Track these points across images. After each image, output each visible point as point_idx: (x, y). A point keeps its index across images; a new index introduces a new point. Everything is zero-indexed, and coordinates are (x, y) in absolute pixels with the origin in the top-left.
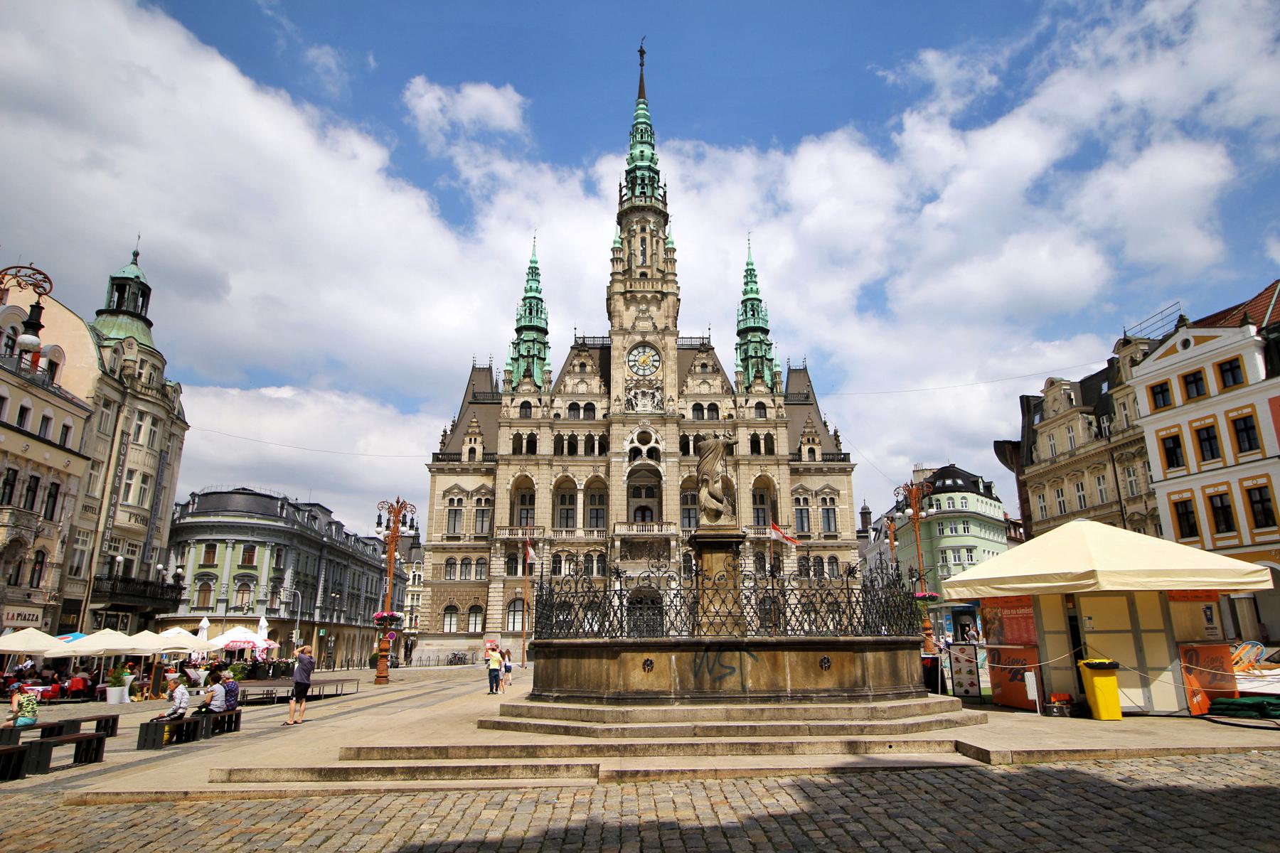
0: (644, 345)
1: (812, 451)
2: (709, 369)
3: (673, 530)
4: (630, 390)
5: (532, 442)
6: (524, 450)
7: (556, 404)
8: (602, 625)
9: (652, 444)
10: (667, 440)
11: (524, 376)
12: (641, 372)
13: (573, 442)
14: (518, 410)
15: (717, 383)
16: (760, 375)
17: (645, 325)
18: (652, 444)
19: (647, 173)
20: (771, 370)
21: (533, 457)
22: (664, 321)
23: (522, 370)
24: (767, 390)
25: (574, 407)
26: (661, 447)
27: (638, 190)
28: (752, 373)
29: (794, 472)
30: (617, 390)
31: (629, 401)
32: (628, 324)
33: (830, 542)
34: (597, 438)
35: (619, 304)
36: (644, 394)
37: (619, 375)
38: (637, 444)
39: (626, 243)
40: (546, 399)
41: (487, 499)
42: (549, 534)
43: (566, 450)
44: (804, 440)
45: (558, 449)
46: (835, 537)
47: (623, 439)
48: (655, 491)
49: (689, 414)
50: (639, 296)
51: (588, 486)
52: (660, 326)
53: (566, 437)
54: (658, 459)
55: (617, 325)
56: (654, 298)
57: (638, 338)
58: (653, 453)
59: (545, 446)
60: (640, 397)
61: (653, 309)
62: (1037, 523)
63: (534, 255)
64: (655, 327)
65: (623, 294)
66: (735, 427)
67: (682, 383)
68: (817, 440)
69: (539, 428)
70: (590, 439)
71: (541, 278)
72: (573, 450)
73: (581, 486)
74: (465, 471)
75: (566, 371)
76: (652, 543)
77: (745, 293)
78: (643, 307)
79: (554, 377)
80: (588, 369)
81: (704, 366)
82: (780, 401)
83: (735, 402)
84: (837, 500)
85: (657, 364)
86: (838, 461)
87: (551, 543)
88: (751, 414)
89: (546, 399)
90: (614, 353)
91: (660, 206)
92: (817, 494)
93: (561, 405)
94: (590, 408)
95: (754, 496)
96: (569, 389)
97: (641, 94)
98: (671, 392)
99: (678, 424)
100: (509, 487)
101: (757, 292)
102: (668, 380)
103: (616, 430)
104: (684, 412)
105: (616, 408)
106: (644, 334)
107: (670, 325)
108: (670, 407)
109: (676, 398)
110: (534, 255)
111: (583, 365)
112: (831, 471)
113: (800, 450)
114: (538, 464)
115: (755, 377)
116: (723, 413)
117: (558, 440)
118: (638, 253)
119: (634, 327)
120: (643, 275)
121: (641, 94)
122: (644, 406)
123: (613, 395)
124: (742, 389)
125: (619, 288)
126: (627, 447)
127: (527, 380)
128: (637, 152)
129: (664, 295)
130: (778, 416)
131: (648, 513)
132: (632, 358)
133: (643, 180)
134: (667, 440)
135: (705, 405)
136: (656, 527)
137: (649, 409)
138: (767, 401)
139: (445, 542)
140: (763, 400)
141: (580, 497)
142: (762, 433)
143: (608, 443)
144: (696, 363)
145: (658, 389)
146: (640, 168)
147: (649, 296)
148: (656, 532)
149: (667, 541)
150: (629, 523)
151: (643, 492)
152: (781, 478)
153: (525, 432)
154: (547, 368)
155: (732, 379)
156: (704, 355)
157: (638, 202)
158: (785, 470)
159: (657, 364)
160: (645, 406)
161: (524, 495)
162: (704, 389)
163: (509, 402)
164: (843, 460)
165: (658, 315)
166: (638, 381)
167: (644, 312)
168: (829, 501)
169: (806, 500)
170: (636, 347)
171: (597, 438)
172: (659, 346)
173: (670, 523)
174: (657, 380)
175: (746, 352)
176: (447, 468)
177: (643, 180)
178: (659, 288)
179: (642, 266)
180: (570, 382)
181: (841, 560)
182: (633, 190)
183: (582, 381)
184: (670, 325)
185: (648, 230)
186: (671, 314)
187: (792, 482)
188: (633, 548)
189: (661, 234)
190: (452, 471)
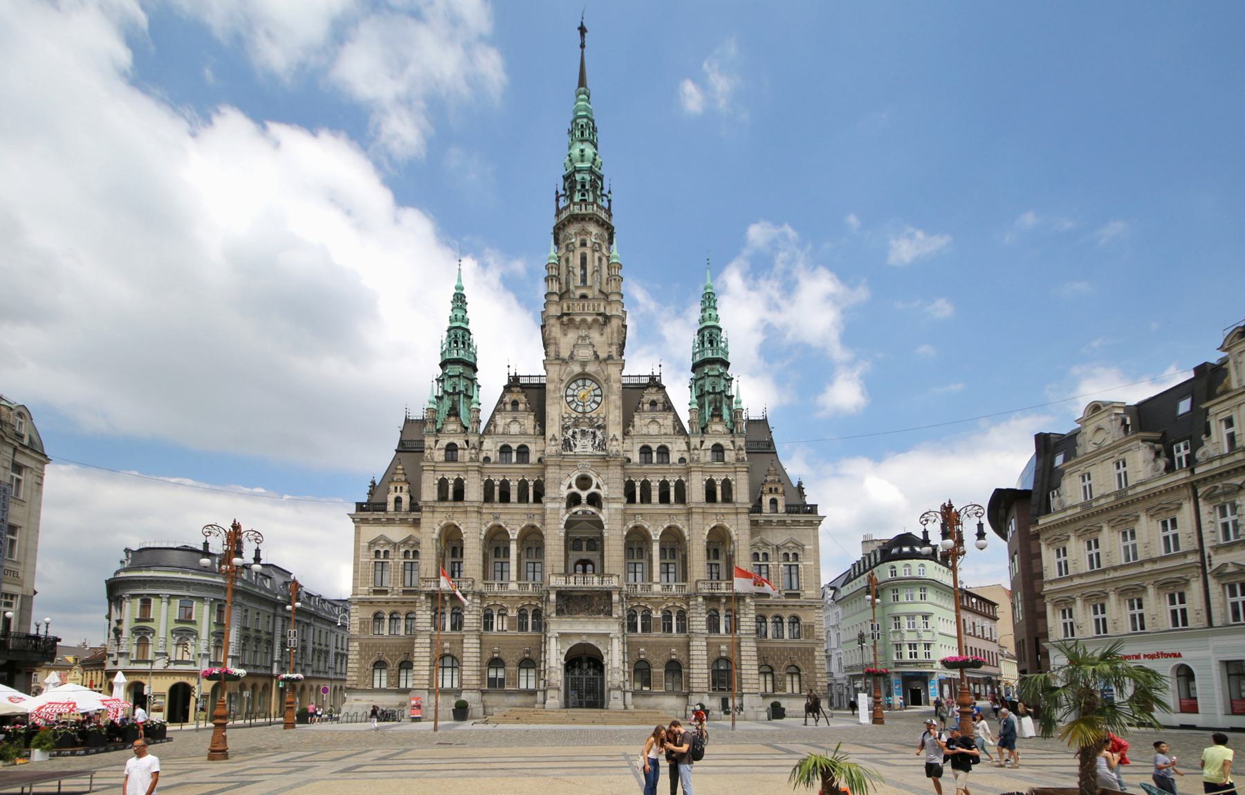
0: (584, 376)
2: (660, 406)
3: (615, 582)
4: (568, 428)
7: (485, 446)
8: (537, 683)
9: (593, 489)
10: (609, 485)
11: (449, 415)
12: (580, 409)
13: (505, 485)
14: (443, 452)
15: (669, 421)
16: (717, 413)
17: (584, 353)
18: (593, 489)
19: (588, 177)
20: (730, 408)
21: (460, 504)
22: (606, 348)
23: (447, 409)
25: (505, 450)
26: (603, 493)
27: (577, 197)
28: (708, 411)
29: (754, 524)
30: (553, 428)
31: (566, 442)
32: (565, 354)
33: (792, 601)
34: (531, 483)
35: (556, 331)
36: (584, 433)
37: (554, 412)
38: (575, 489)
39: (563, 262)
40: (474, 439)
41: (412, 552)
42: (480, 586)
44: (766, 489)
45: (488, 498)
46: (798, 595)
47: (561, 485)
48: (596, 544)
49: (636, 457)
50: (578, 319)
52: (603, 355)
53: (497, 483)
54: (600, 507)
55: (552, 354)
56: (595, 321)
57: (577, 369)
58: (594, 500)
59: (474, 492)
60: (578, 436)
61: (595, 336)
62: (1051, 582)
64: (597, 357)
66: (688, 472)
67: (627, 422)
68: (780, 490)
69: (466, 472)
70: (523, 486)
71: (468, 308)
72: (505, 498)
73: (514, 535)
75: (497, 410)
76: (592, 597)
77: (703, 320)
78: (583, 333)
79: (485, 417)
80: (521, 407)
81: (653, 403)
82: (740, 442)
83: (688, 444)
84: (800, 557)
86: (803, 511)
87: (481, 595)
88: (708, 456)
89: (474, 439)
91: (603, 215)
92: (778, 548)
93: (491, 447)
94: (523, 451)
95: (708, 550)
96: (500, 429)
97: (582, 82)
98: (615, 430)
99: (622, 466)
100: (435, 536)
101: (717, 319)
102: (611, 417)
103: (551, 473)
104: (629, 455)
105: (552, 449)
107: (614, 354)
108: (613, 447)
109: (620, 437)
111: (515, 404)
112: (796, 523)
113: (760, 499)
114: (466, 512)
115: (712, 416)
116: (674, 457)
117: (489, 486)
118: (578, 272)
119: (572, 357)
121: (582, 82)
122: (584, 446)
123: (549, 434)
124: (697, 428)
125: (554, 310)
126: (565, 492)
127: (452, 419)
128: (576, 152)
129: (607, 319)
130: (738, 460)
131: (589, 567)
132: (570, 392)
133: (583, 186)
134: (609, 485)
135: (654, 447)
136: (596, 579)
137: (590, 450)
138: (726, 442)
140: (722, 442)
141: (513, 548)
142: (718, 479)
143: (543, 490)
144: (644, 400)
145: (599, 427)
146: (580, 171)
147: (589, 319)
148: (596, 584)
149: (609, 594)
150: (566, 573)
151: (584, 544)
152: (739, 529)
153: (451, 478)
154: (475, 406)
155: (685, 418)
156: (654, 390)
157: (576, 210)
158: (744, 520)
160: (584, 447)
161: (452, 543)
162: (654, 429)
163: (433, 444)
164: (810, 512)
165: (601, 341)
166: (577, 419)
167: (584, 338)
168: (792, 557)
169: (766, 555)
170: (574, 379)
171: (531, 483)
172: (601, 378)
173: (611, 576)
175: (702, 386)
177: (583, 186)
180: (500, 421)
181: (803, 621)
182: (571, 198)
183: (515, 420)
184: (614, 354)
185: (589, 244)
186: (615, 341)
187: (752, 535)
188: (571, 602)
189: (604, 250)
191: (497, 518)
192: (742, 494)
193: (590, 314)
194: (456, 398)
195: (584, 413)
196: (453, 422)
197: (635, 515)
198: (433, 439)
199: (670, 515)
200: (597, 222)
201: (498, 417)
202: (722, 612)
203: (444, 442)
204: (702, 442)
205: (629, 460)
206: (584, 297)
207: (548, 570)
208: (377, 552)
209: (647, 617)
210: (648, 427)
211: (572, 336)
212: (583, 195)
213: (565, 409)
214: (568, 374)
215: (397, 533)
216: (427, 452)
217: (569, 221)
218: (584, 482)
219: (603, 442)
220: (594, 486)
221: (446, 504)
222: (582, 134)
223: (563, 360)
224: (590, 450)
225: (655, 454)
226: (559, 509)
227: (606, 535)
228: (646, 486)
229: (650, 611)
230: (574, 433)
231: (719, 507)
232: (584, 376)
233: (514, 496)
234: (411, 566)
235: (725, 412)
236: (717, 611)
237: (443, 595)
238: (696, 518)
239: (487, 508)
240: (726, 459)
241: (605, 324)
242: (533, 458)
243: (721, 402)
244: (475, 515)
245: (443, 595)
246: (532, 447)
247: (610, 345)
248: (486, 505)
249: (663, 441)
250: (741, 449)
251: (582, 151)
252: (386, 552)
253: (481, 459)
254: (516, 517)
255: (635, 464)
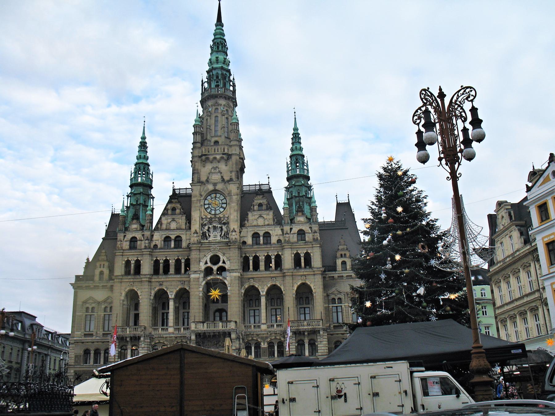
0: (215, 191)
1: (344, 263)
2: (264, 207)
3: (232, 326)
4: (205, 225)
5: (138, 264)
6: (132, 272)
7: (155, 238)
9: (221, 264)
11: (133, 219)
12: (213, 212)
13: (167, 262)
14: (128, 243)
15: (269, 216)
16: (300, 210)
17: (216, 177)
18: (221, 264)
21: (138, 277)
22: (229, 174)
24: (306, 220)
25: (167, 239)
26: (227, 266)
30: (196, 226)
32: (203, 179)
38: (209, 264)
40: (147, 234)
42: (150, 330)
43: (161, 271)
45: (156, 271)
47: (201, 262)
49: (249, 241)
50: (211, 157)
51: (177, 295)
52: (227, 178)
53: (161, 261)
56: (222, 158)
57: (211, 187)
58: (222, 270)
59: (147, 268)
60: (211, 230)
61: (222, 166)
63: (144, 133)
65: (200, 157)
66: (283, 249)
70: (178, 262)
74: (96, 287)
78: (215, 165)
80: (178, 211)
81: (260, 205)
82: (316, 228)
83: (282, 230)
85: (224, 206)
88: (294, 238)
90: (193, 199)
93: (158, 238)
94: (178, 240)
96: (164, 227)
98: (234, 225)
99: (240, 249)
103: (194, 255)
104: (245, 240)
105: (195, 239)
106: (215, 184)
108: (234, 236)
110: (144, 133)
115: (297, 211)
116: (274, 240)
120: (216, 142)
124: (287, 220)
126: (203, 266)
127: (135, 221)
130: (314, 239)
132: (206, 202)
133: (217, 77)
134: (231, 261)
135: (261, 233)
138: (306, 228)
139: (83, 338)
145: (224, 224)
147: (218, 157)
148: (220, 328)
152: (316, 285)
157: (214, 92)
159: (224, 206)
160: (215, 236)
162: (261, 222)
163: (122, 238)
167: (215, 168)
170: (210, 194)
172: (226, 193)
174: (224, 217)
175: (291, 193)
176: (84, 285)
177: (217, 77)
178: (226, 151)
179: (215, 136)
180: (164, 221)
183: (173, 220)
184: (234, 177)
190: (88, 288)
191: (161, 285)
192: (317, 261)
193: (219, 154)
194: (138, 207)
195: (215, 214)
196: (135, 224)
197: (249, 279)
198: (123, 235)
199: (272, 277)
200: (225, 98)
201: (163, 218)
202: (306, 341)
203: (129, 236)
204: (291, 229)
205: (244, 243)
206: (216, 142)
207: (192, 319)
208: (87, 308)
209: (258, 346)
210: (259, 220)
211: (209, 166)
212: (217, 82)
213: (204, 214)
214: (205, 191)
215: (100, 295)
216: (119, 243)
217: (208, 99)
218: (215, 259)
219: (227, 233)
220: (221, 262)
221: (129, 277)
222: (218, 47)
223: (202, 183)
224: (219, 238)
225: (261, 238)
226: (199, 278)
227: (229, 294)
228: (256, 259)
229: (260, 344)
230: (209, 228)
231: (302, 272)
232: (215, 191)
233: (172, 270)
234: (107, 318)
235: (306, 208)
236: (303, 341)
237: (126, 338)
238: (288, 279)
239: (155, 279)
240: (307, 239)
241: (228, 159)
242: (184, 244)
243: (303, 202)
244: (147, 283)
245: (126, 338)
246: (184, 237)
247: (231, 172)
248: (155, 277)
249: (267, 229)
250: (315, 232)
251: (217, 58)
252: (93, 308)
253: (152, 246)
254: (174, 283)
255: (250, 245)
